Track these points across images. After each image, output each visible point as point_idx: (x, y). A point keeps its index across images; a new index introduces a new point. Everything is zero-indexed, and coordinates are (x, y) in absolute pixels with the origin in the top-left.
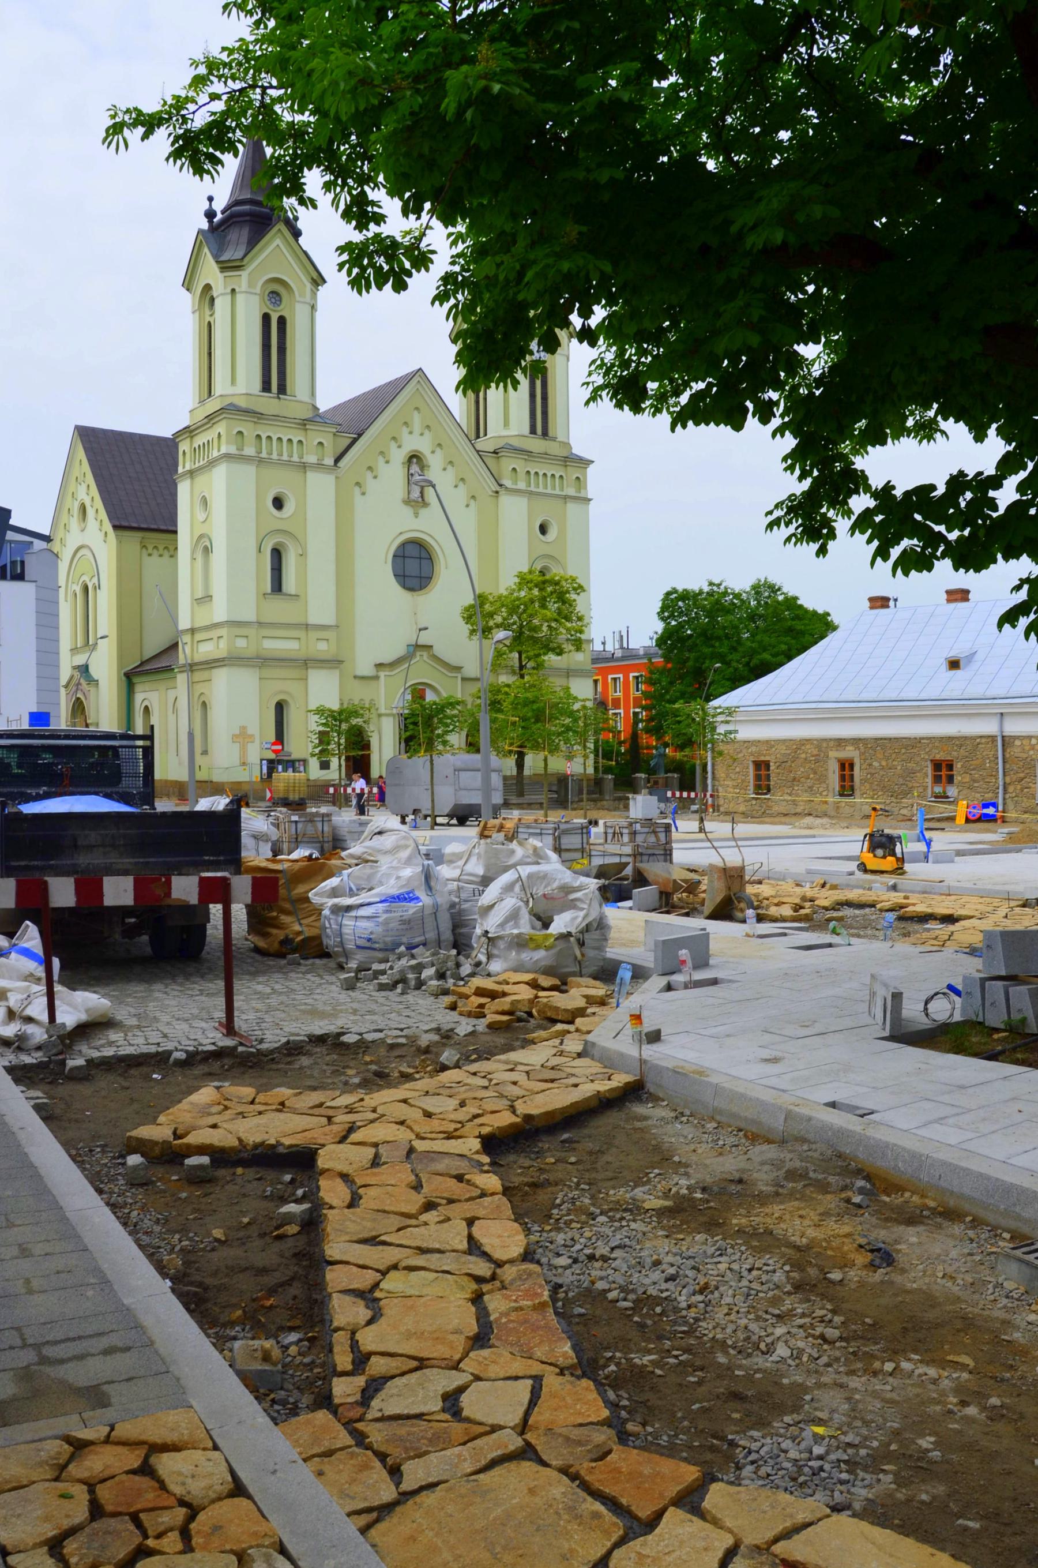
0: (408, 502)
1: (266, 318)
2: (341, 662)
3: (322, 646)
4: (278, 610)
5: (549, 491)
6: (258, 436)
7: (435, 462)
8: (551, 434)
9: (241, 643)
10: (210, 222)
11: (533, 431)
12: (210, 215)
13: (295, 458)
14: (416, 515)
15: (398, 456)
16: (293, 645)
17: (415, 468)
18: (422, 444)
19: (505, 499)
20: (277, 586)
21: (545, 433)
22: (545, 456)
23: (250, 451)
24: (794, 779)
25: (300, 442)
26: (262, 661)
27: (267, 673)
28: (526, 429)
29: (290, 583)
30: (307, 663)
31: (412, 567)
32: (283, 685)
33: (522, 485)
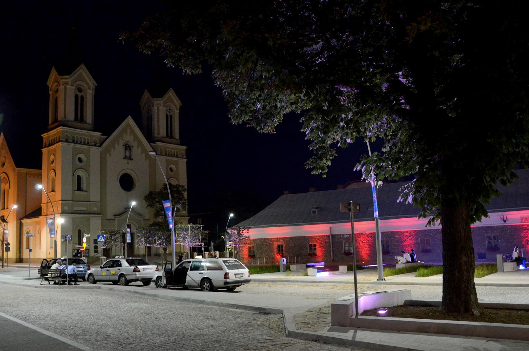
0: (125, 158)
3: (95, 209)
9: (66, 208)
14: (128, 163)
15: (122, 142)
20: (79, 189)
24: (262, 252)
28: (165, 135)
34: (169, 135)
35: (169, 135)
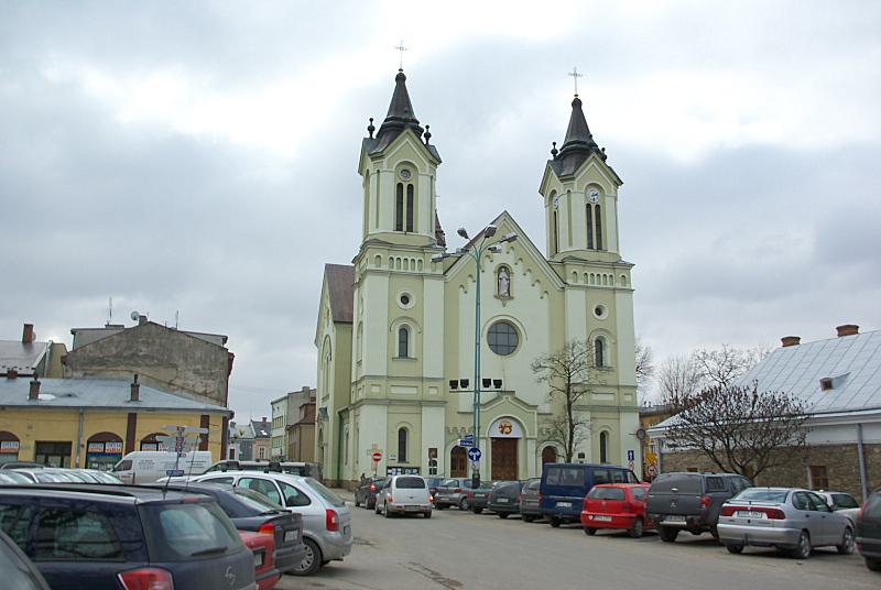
0: (498, 297)
1: (400, 186)
2: (446, 402)
4: (403, 368)
5: (602, 286)
6: (392, 258)
7: (517, 270)
8: (603, 248)
10: (371, 134)
11: (590, 246)
12: (371, 129)
13: (417, 271)
14: (504, 305)
15: (490, 268)
16: (414, 391)
17: (503, 275)
18: (509, 260)
19: (569, 292)
20: (404, 353)
21: (599, 248)
22: (598, 263)
23: (385, 267)
25: (420, 261)
26: (389, 402)
27: (392, 409)
28: (584, 245)
29: (412, 353)
30: (420, 403)
31: (502, 339)
32: (403, 417)
33: (581, 283)
34: (595, 247)
35: (595, 247)
